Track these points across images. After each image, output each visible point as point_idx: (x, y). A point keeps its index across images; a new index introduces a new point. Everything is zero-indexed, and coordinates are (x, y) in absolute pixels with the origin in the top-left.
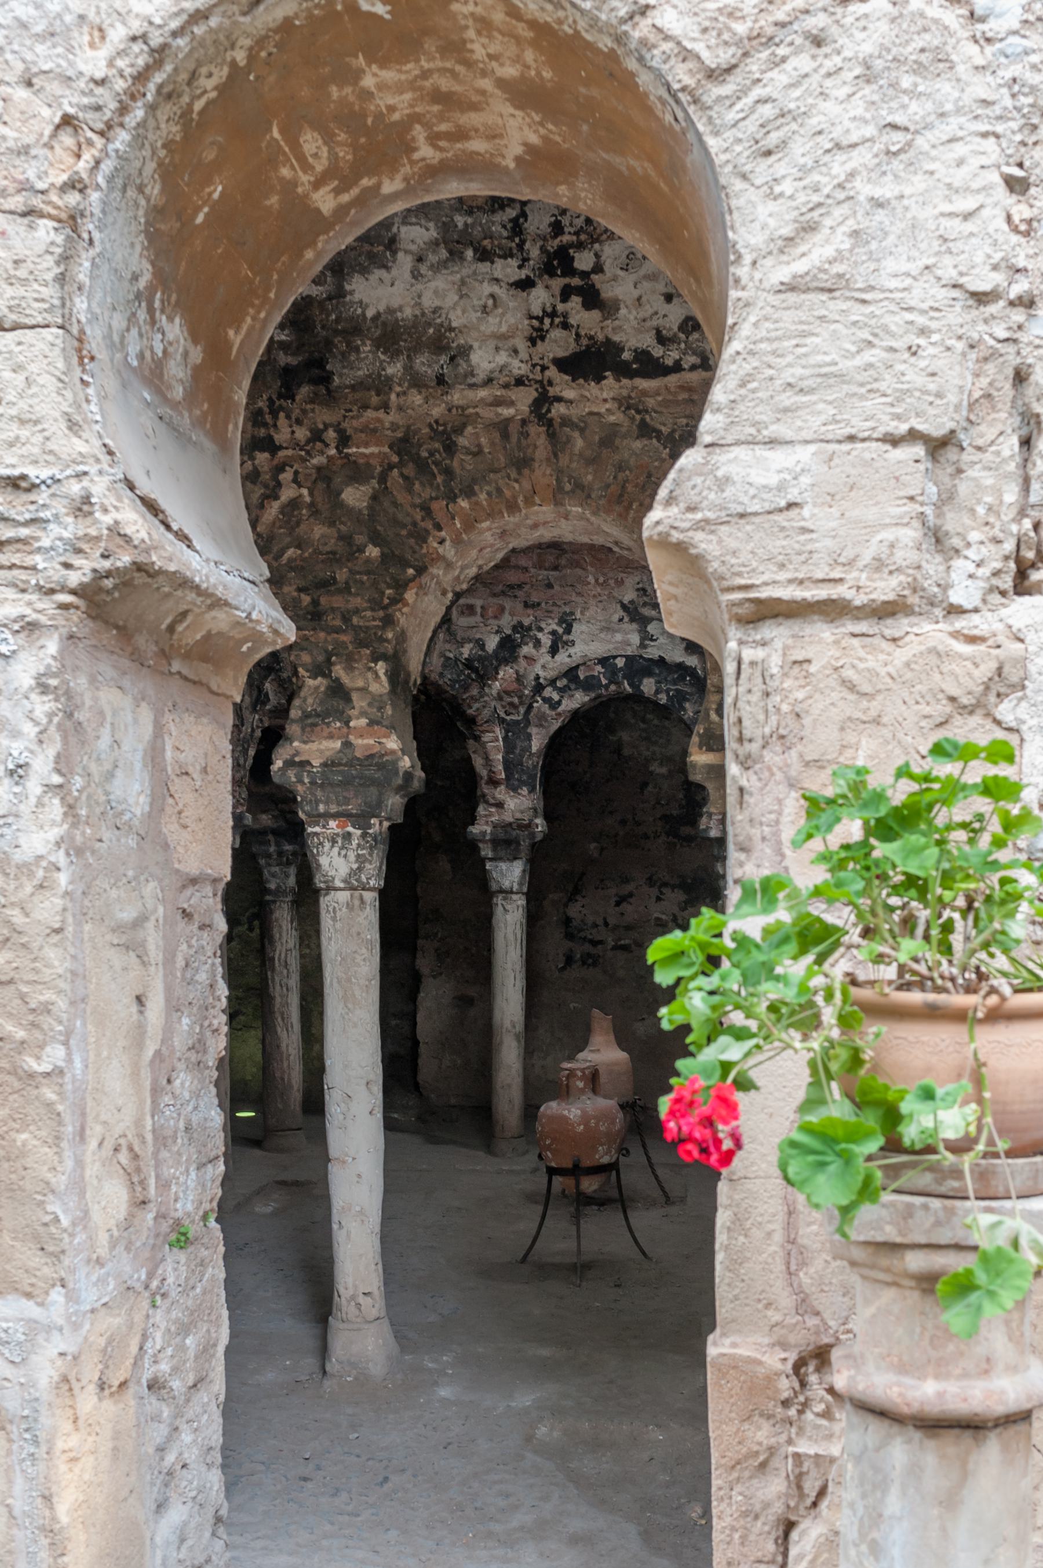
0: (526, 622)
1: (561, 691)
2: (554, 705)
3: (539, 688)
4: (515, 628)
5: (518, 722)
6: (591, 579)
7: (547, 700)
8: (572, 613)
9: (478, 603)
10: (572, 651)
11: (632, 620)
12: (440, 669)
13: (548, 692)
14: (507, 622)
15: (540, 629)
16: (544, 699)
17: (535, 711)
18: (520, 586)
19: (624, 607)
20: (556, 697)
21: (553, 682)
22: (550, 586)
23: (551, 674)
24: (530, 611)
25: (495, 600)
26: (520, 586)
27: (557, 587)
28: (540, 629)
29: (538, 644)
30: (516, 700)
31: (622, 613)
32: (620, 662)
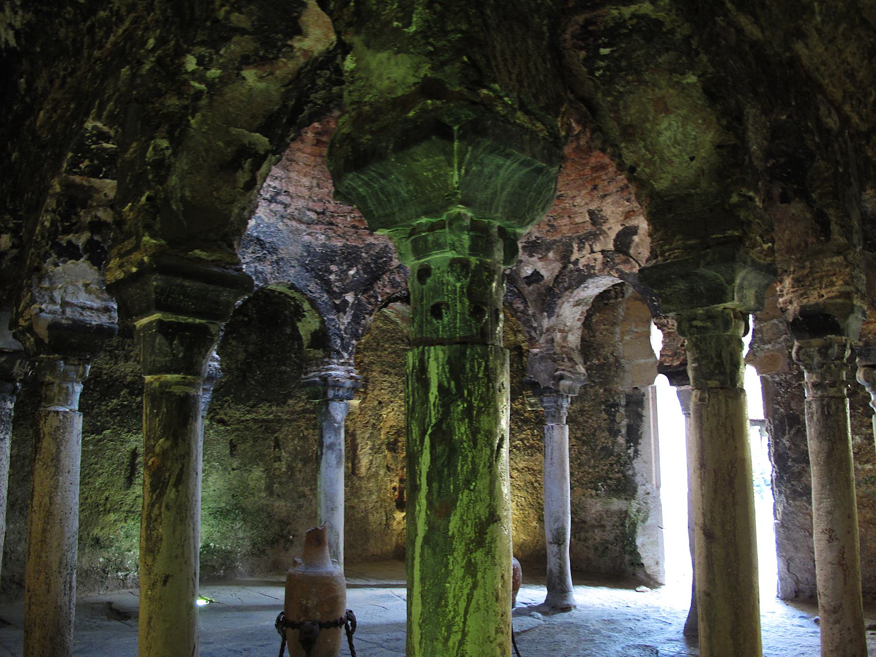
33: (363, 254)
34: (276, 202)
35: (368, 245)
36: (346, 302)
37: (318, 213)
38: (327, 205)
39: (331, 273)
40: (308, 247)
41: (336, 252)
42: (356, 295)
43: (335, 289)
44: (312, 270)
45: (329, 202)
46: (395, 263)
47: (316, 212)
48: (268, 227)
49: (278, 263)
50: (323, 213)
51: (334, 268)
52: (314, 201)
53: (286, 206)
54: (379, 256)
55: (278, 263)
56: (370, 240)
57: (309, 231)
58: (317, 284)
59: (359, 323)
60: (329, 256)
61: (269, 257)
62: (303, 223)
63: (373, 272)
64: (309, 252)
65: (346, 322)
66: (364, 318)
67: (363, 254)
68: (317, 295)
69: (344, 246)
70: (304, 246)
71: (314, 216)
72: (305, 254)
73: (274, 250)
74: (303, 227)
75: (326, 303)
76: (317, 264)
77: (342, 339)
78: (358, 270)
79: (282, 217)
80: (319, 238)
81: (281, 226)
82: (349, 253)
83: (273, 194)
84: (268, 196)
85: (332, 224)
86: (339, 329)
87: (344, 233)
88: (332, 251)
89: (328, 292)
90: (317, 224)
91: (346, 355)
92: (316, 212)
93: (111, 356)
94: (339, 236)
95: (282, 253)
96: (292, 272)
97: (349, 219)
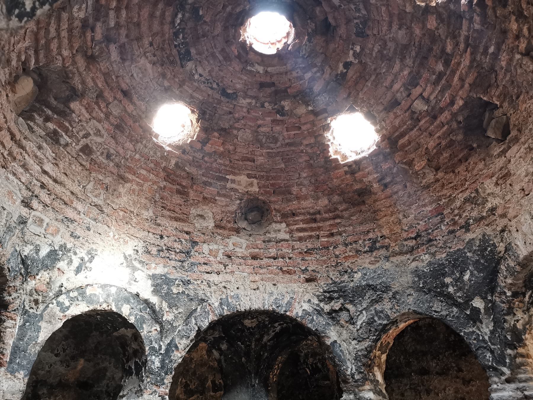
0: (69, 246)
1: (72, 299)
2: (64, 309)
3: (59, 294)
4: (61, 246)
5: (36, 316)
6: (111, 234)
7: (58, 304)
8: (96, 250)
9: (47, 220)
10: (88, 273)
11: (128, 266)
12: (8, 256)
13: (62, 298)
14: (58, 241)
15: (75, 254)
16: (58, 304)
17: (49, 310)
18: (72, 221)
19: (125, 257)
20: (67, 303)
21: (69, 291)
22: (89, 229)
23: (69, 286)
24: (72, 239)
25: (56, 223)
26: (72, 221)
27: (92, 231)
28: (75, 254)
29: (71, 262)
30: (40, 298)
31: (122, 260)
32: (113, 290)
33: (468, 254)
34: (376, 249)
35: (468, 242)
36: (476, 311)
37: (415, 238)
38: (419, 227)
39: (447, 286)
40: (416, 272)
41: (443, 264)
42: (484, 298)
43: (459, 300)
44: (430, 290)
45: (418, 224)
46: (501, 247)
47: (412, 238)
48: (375, 272)
49: (395, 298)
50: (418, 236)
51: (448, 280)
52: (405, 231)
53: (387, 248)
54: (482, 249)
55: (395, 298)
56: (469, 236)
57: (412, 258)
58: (442, 302)
59: (503, 328)
60: (438, 272)
61: (385, 295)
62: (406, 253)
63: (486, 268)
64: (418, 276)
65: (487, 331)
66: (505, 321)
67: (468, 254)
68: (444, 313)
69: (448, 255)
70: (412, 273)
71: (412, 243)
72: (416, 279)
73: (387, 288)
74: (408, 256)
75: (458, 317)
76: (431, 283)
77: (492, 352)
78: (471, 272)
79: (387, 258)
80: (424, 260)
81: (387, 265)
82: (456, 260)
83: (370, 245)
84: (367, 248)
85: (430, 240)
86: (484, 340)
87: (445, 242)
88: (440, 265)
89: (456, 306)
90: (418, 248)
91: (505, 370)
92: (412, 238)
93: (416, 392)
94: (441, 247)
95: (396, 287)
96: (411, 300)
97: (443, 228)
